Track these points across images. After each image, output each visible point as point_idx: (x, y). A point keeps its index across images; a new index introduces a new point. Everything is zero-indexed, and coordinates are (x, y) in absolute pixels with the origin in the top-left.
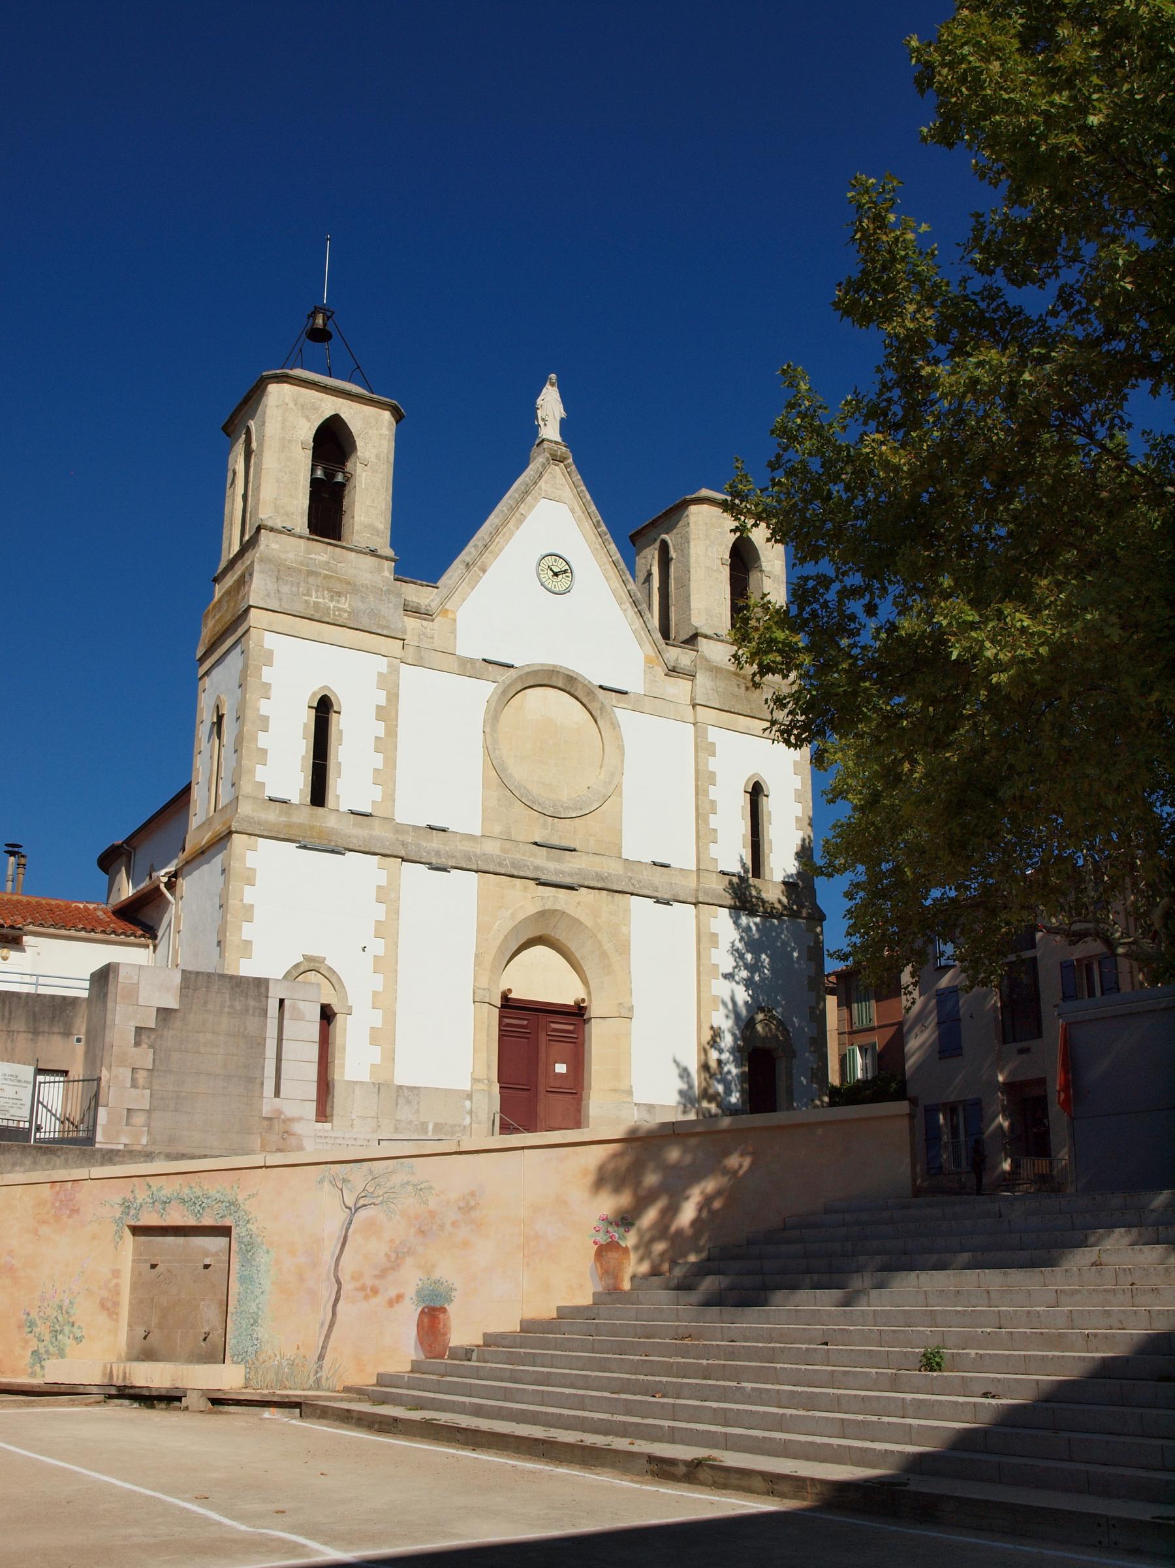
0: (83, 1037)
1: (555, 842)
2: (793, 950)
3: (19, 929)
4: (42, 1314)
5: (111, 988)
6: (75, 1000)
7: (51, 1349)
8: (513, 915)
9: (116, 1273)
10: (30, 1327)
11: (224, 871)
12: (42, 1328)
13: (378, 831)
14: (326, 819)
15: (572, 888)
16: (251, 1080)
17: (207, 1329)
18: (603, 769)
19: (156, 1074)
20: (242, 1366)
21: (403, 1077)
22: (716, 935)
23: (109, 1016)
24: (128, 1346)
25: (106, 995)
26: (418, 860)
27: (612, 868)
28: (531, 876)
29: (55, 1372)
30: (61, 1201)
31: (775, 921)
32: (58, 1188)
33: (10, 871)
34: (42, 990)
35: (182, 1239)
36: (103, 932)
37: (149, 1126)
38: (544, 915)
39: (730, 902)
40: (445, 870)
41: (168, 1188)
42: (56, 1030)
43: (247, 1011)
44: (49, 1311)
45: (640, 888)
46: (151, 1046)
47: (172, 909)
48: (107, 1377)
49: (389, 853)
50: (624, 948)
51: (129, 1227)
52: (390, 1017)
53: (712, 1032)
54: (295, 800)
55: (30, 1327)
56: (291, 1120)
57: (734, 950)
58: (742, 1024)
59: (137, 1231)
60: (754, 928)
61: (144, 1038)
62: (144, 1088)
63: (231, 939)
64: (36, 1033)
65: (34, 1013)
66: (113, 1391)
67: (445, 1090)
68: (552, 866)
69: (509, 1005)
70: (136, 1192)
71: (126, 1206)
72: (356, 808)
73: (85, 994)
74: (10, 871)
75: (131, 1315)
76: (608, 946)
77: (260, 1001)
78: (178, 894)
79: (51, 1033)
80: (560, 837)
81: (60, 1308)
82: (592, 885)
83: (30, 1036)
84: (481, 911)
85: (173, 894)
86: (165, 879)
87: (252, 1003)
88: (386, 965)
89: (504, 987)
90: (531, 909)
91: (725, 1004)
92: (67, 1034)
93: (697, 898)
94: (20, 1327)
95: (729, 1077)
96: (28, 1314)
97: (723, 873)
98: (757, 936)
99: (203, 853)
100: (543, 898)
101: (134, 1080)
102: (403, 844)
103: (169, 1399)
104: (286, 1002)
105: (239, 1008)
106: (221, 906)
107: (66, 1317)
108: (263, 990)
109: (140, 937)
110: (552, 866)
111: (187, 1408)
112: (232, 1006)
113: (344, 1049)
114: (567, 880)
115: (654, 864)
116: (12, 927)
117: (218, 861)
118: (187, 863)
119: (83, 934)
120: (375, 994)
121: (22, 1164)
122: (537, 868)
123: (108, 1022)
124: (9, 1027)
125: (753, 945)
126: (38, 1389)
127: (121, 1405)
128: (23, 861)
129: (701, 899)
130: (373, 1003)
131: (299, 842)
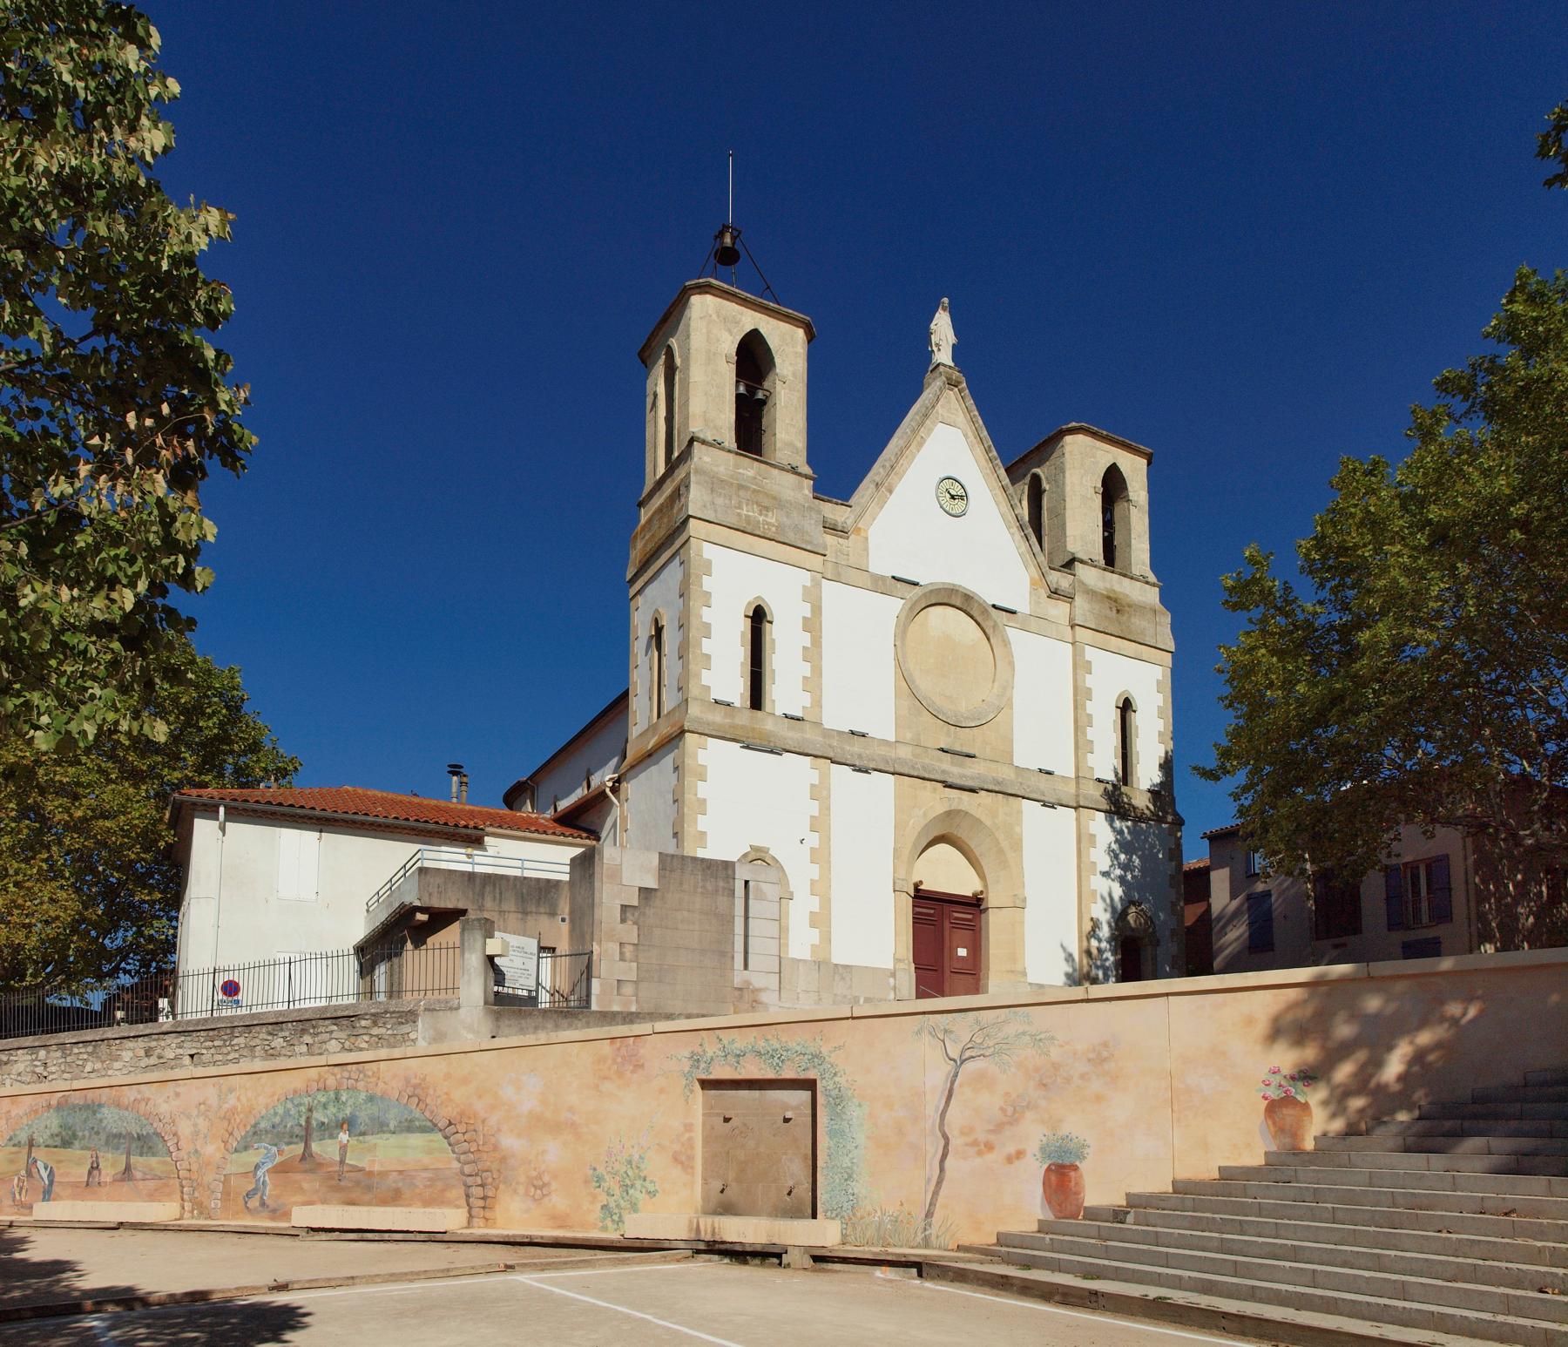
0: (567, 917)
1: (957, 748)
2: (1159, 851)
3: (482, 829)
4: (609, 1169)
5: (597, 869)
6: (556, 884)
7: (622, 1203)
8: (925, 814)
9: (689, 1127)
10: (597, 1181)
11: (676, 769)
12: (609, 1182)
13: (809, 736)
14: (766, 723)
15: (973, 790)
16: (723, 954)
17: (791, 1183)
18: (996, 683)
19: (641, 948)
20: (837, 1222)
21: (839, 957)
22: (1094, 836)
23: (597, 894)
24: (703, 1199)
25: (592, 875)
26: (844, 761)
27: (1005, 774)
28: (939, 779)
29: (636, 1227)
30: (623, 1057)
31: (1144, 825)
32: (618, 1045)
33: (454, 789)
34: (527, 874)
35: (758, 1092)
36: (554, 834)
37: (636, 995)
38: (950, 814)
39: (1105, 806)
40: (866, 772)
41: (740, 1041)
42: (542, 910)
43: (717, 891)
44: (617, 1166)
45: (1031, 792)
46: (635, 923)
47: (616, 812)
48: (694, 1231)
49: (820, 754)
50: (1017, 845)
51: (698, 1080)
52: (826, 903)
53: (1091, 924)
54: (737, 704)
55: (597, 1181)
56: (760, 990)
57: (1110, 851)
58: (1117, 916)
59: (706, 1084)
60: (1126, 831)
61: (628, 914)
62: (631, 961)
63: (688, 830)
64: (525, 913)
65: (522, 894)
66: (702, 1246)
67: (873, 968)
68: (955, 770)
69: (921, 897)
70: (706, 1045)
71: (696, 1060)
72: (789, 713)
73: (566, 878)
74: (454, 789)
75: (705, 1170)
76: (1004, 844)
77: (728, 882)
78: (622, 796)
79: (538, 913)
80: (962, 745)
81: (630, 1162)
82: (990, 788)
83: (520, 916)
84: (899, 809)
85: (618, 798)
86: (610, 784)
87: (721, 884)
88: (821, 856)
89: (916, 879)
90: (940, 809)
91: (1103, 899)
92: (552, 914)
93: (1078, 802)
94: (586, 1182)
95: (1107, 964)
96: (595, 1169)
97: (1099, 781)
98: (1129, 838)
99: (650, 755)
100: (949, 799)
101: (622, 954)
102: (830, 746)
103: (769, 1256)
104: (751, 884)
105: (710, 888)
106: (675, 801)
107: (637, 1171)
108: (730, 872)
109: (586, 838)
110: (955, 770)
111: (789, 1265)
112: (702, 887)
113: (788, 929)
114: (970, 783)
115: (1041, 770)
116: (475, 828)
117: (668, 761)
118: (632, 767)
119: (536, 835)
120: (813, 882)
121: (544, 1028)
122: (943, 772)
123: (596, 900)
124: (500, 907)
125: (1125, 846)
126: (618, 1245)
127: (710, 1261)
128: (465, 780)
129: (1082, 804)
130: (811, 890)
131: (743, 742)
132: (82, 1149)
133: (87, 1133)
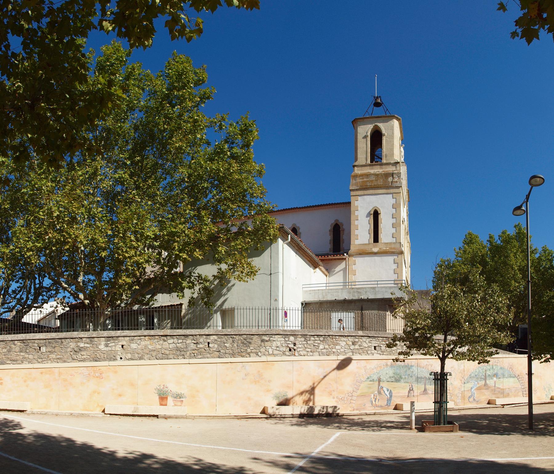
132: (405, 383)
133: (407, 377)
